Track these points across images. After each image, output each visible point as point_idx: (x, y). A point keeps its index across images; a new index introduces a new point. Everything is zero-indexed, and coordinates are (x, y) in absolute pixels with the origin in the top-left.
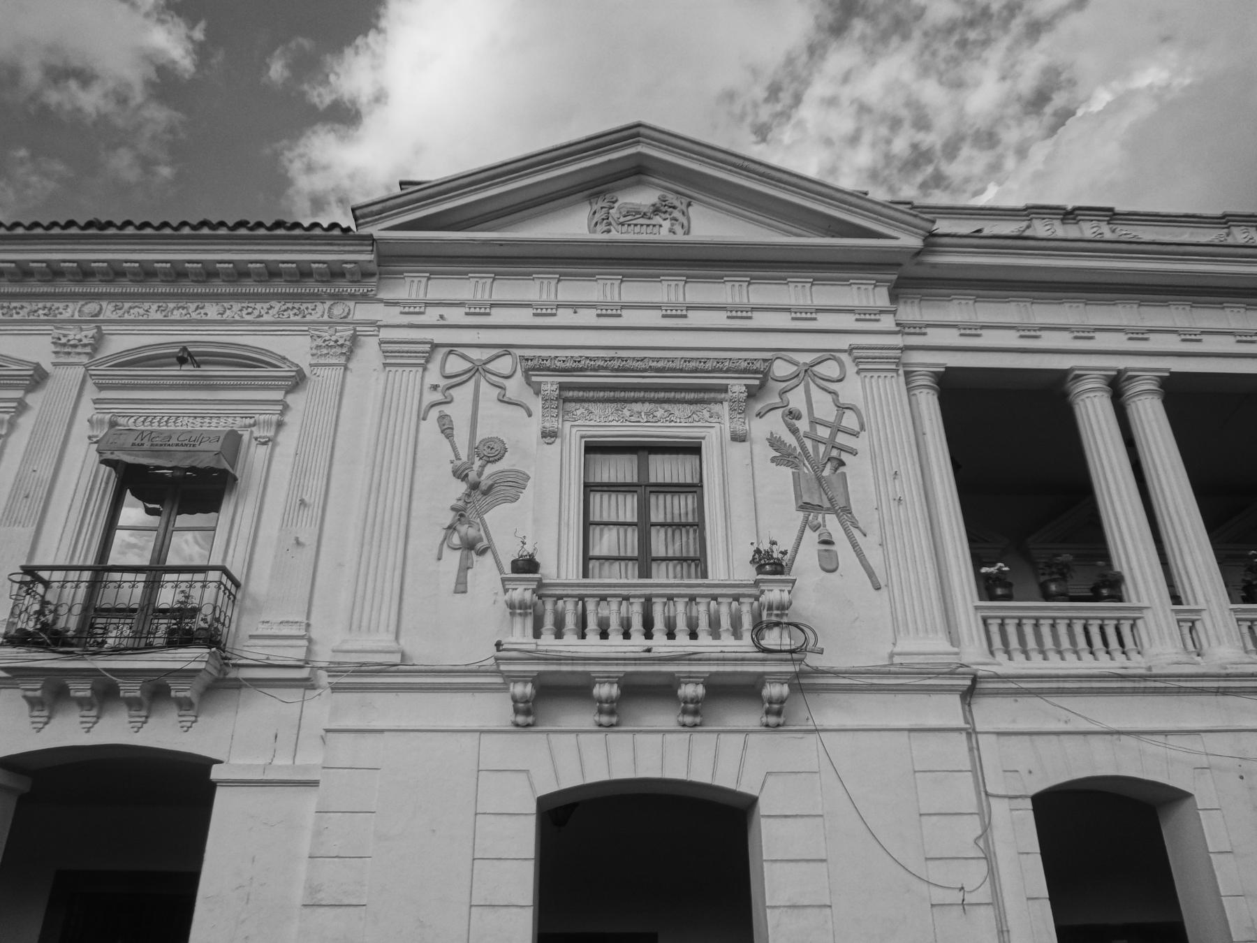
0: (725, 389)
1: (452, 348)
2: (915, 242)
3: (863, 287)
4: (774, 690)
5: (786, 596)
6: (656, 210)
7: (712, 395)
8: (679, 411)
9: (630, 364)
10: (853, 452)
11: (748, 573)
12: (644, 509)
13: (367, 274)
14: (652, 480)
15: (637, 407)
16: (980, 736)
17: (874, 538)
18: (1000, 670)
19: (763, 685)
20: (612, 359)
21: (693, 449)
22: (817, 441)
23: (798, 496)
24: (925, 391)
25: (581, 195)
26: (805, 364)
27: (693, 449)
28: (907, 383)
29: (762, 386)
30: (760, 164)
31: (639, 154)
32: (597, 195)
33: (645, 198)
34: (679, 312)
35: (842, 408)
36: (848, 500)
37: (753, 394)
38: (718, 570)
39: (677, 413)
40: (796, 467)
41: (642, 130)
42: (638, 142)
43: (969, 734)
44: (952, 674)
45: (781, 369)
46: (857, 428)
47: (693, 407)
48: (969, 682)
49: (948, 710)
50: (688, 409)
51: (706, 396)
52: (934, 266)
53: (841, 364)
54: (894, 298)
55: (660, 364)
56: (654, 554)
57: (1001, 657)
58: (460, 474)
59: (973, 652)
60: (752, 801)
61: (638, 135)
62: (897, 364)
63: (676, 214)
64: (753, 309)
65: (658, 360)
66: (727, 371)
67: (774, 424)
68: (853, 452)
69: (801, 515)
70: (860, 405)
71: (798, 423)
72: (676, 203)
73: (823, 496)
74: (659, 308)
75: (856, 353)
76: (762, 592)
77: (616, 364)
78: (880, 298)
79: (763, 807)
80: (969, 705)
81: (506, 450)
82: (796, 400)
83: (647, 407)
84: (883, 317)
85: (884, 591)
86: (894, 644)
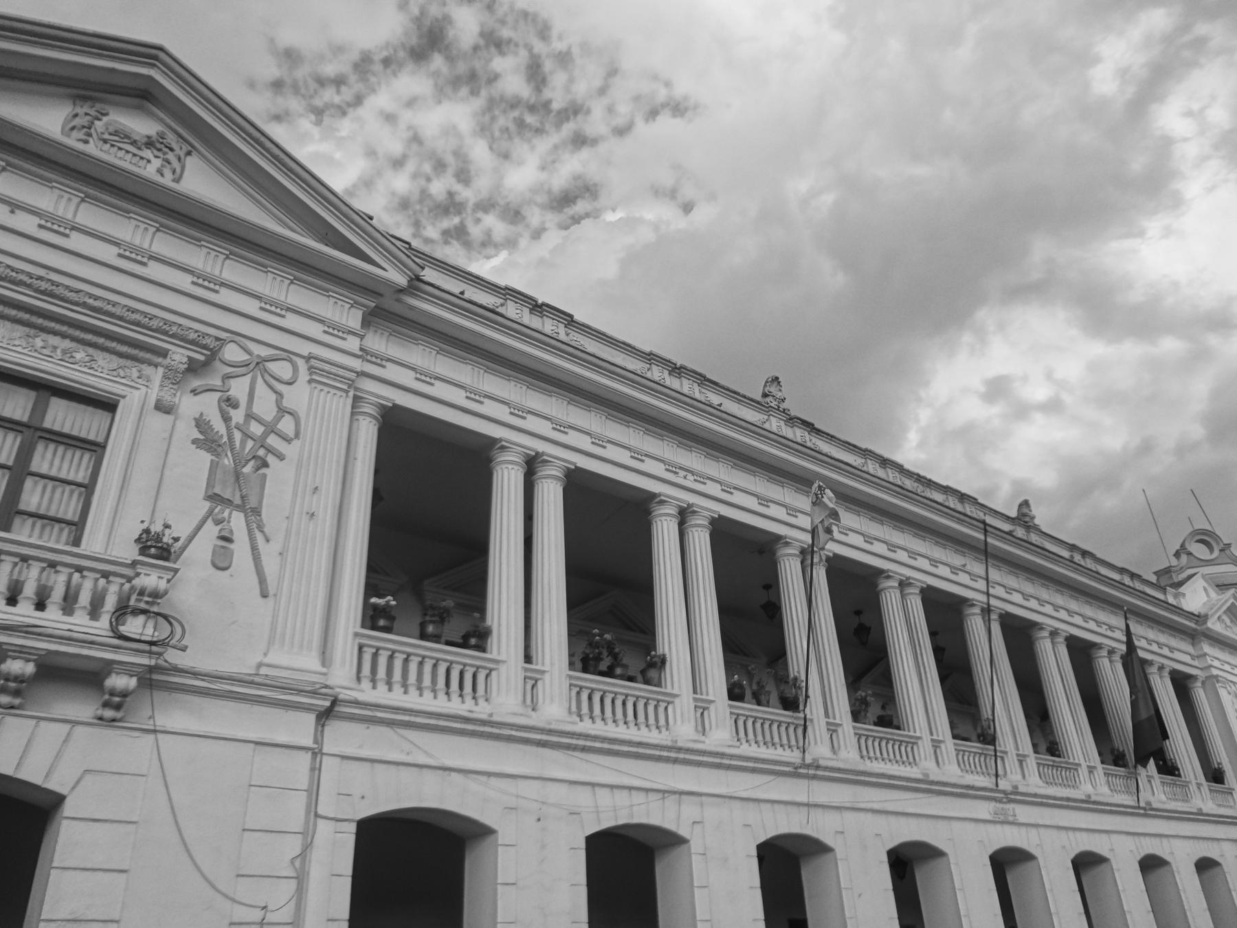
0: (164, 354)
2: (402, 280)
3: (340, 303)
4: (118, 681)
5: (162, 585)
6: (149, 143)
7: (148, 356)
8: (104, 361)
9: (60, 291)
10: (281, 457)
11: (129, 552)
12: (25, 454)
14: (47, 424)
15: (54, 340)
16: (325, 758)
17: (275, 546)
18: (361, 697)
19: (109, 674)
20: (40, 278)
21: (108, 405)
22: (247, 435)
23: (210, 484)
24: (369, 419)
25: (69, 91)
26: (258, 356)
27: (108, 405)
28: (353, 407)
29: (207, 364)
30: (277, 146)
31: (150, 78)
32: (85, 99)
33: (141, 126)
34: (139, 258)
35: (282, 411)
36: (260, 502)
37: (194, 368)
38: (94, 542)
39: (100, 362)
40: (218, 455)
41: (162, 55)
42: (154, 65)
43: (315, 754)
44: (314, 693)
45: (232, 353)
46: (291, 434)
47: (123, 362)
48: (328, 704)
49: (301, 728)
50: (116, 362)
51: (142, 354)
52: (412, 308)
53: (295, 369)
54: (366, 323)
55: (97, 304)
56: (22, 507)
57: (366, 684)
59: (341, 677)
60: (58, 800)
61: (156, 58)
62: (350, 386)
63: (170, 156)
64: (222, 284)
65: (96, 298)
66: (172, 336)
67: (208, 405)
68: (281, 457)
69: (207, 505)
70: (302, 415)
71: (232, 412)
72: (174, 146)
73: (235, 491)
74: (117, 244)
75: (313, 362)
76: (138, 575)
77: (44, 285)
78: (354, 319)
79: (68, 809)
80: (323, 726)
82: (238, 389)
83: (67, 344)
84: (350, 338)
85: (270, 601)
86: (265, 655)
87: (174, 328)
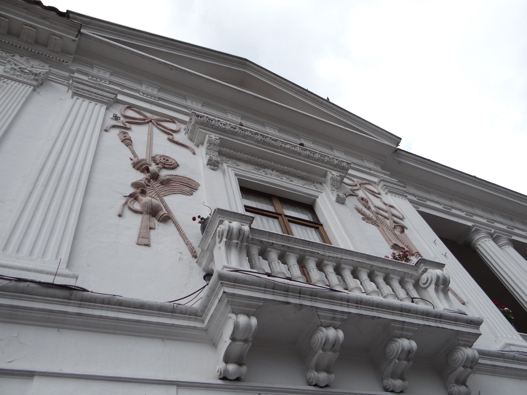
1: (130, 107)
13: (64, 51)
52: (400, 162)
55: (287, 146)
58: (140, 166)
61: (245, 65)
66: (327, 163)
75: (382, 183)
77: (259, 137)
81: (178, 166)
83: (275, 173)
87: (327, 158)
